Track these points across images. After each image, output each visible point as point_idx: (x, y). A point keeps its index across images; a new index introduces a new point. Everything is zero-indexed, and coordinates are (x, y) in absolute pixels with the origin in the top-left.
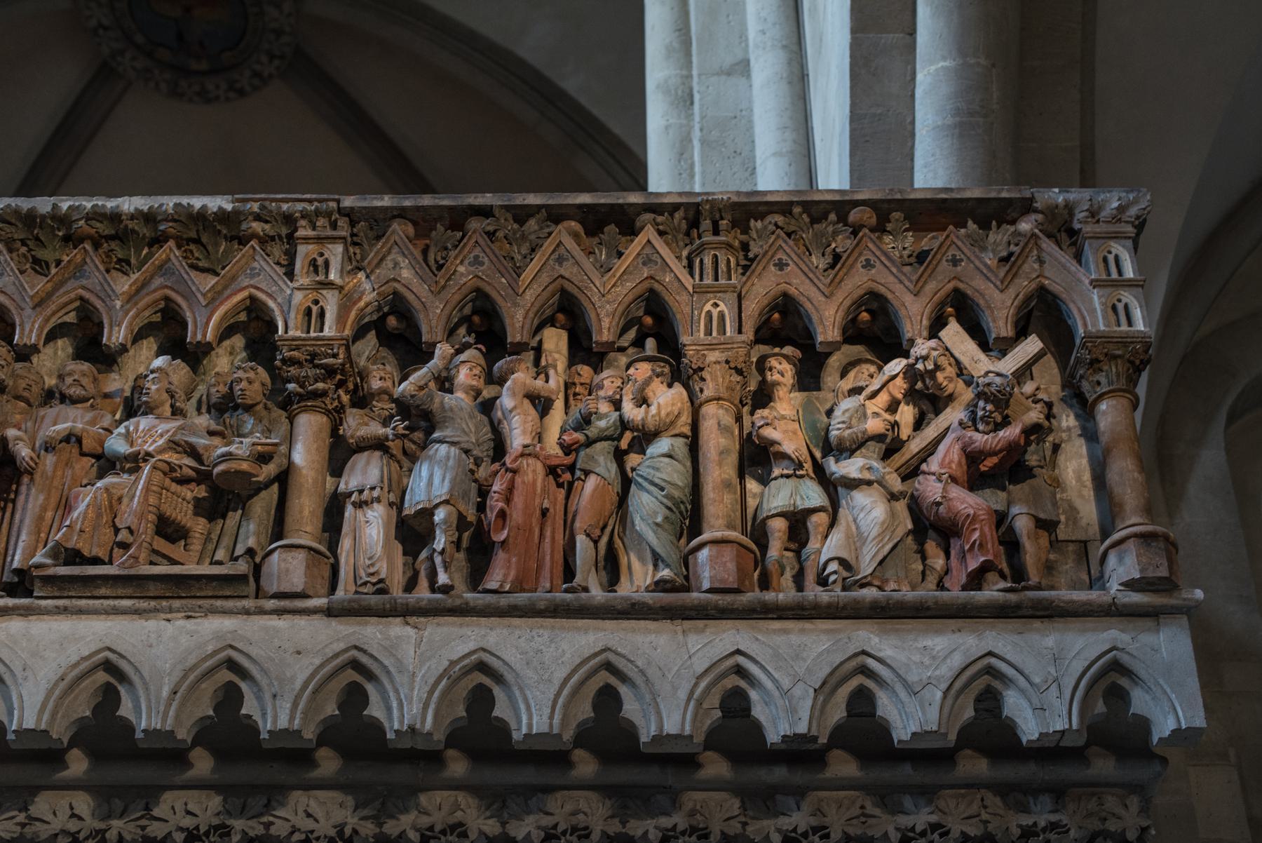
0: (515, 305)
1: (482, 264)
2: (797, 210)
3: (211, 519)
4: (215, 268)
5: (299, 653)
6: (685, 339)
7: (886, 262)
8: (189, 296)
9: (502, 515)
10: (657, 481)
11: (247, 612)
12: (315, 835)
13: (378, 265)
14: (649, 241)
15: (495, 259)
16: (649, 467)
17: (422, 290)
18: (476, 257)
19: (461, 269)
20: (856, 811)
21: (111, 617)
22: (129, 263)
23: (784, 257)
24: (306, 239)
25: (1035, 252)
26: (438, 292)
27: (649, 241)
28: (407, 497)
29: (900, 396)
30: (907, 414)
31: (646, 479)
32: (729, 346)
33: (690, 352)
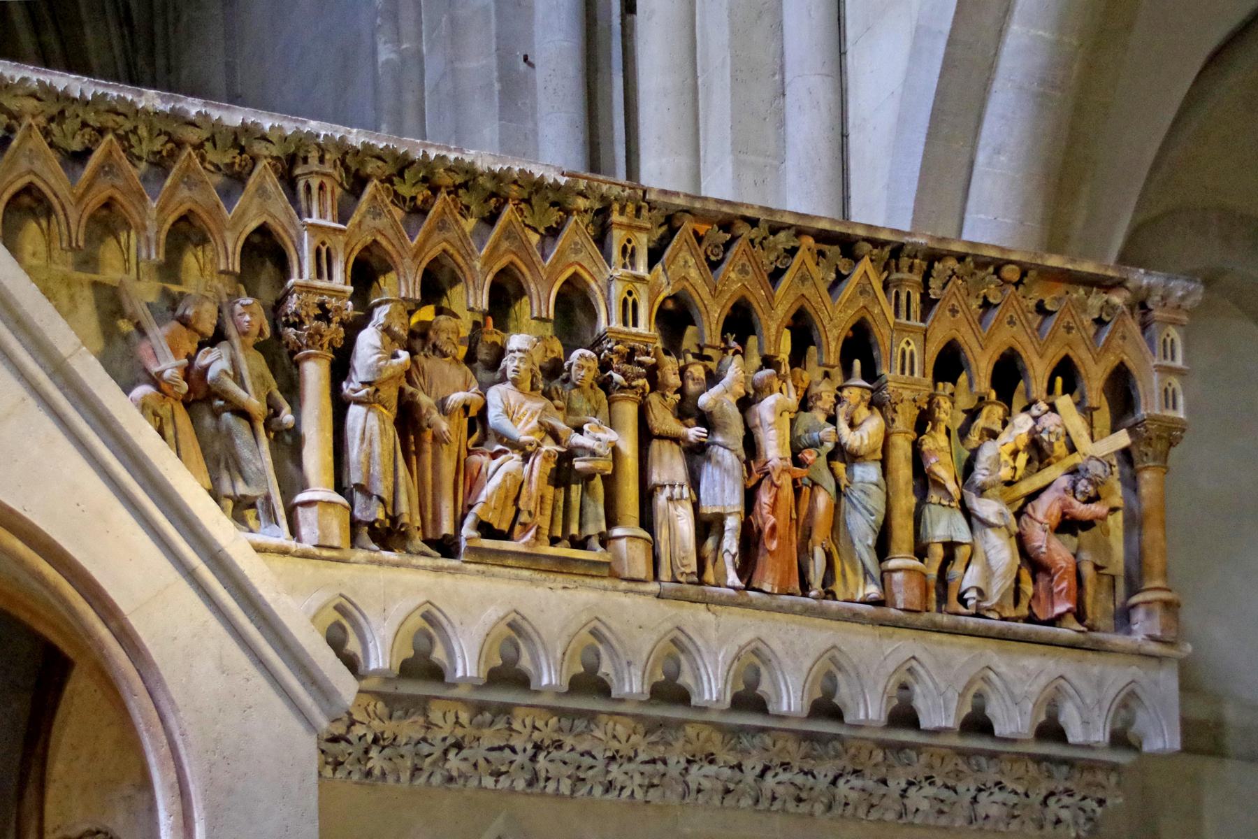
0: (771, 317)
1: (747, 273)
2: (969, 259)
3: (556, 486)
4: (538, 227)
5: (640, 627)
6: (883, 371)
7: (1024, 321)
8: (532, 266)
9: (773, 528)
10: (869, 507)
11: (605, 589)
12: (620, 754)
13: (673, 262)
14: (865, 272)
15: (757, 271)
16: (862, 491)
17: (704, 291)
18: (743, 265)
19: (733, 275)
20: (950, 767)
21: (514, 582)
22: (468, 208)
23: (956, 304)
24: (620, 225)
25: (1121, 329)
26: (715, 292)
27: (865, 272)
28: (702, 496)
29: (1021, 447)
30: (1022, 458)
31: (860, 502)
32: (918, 387)
33: (891, 386)
